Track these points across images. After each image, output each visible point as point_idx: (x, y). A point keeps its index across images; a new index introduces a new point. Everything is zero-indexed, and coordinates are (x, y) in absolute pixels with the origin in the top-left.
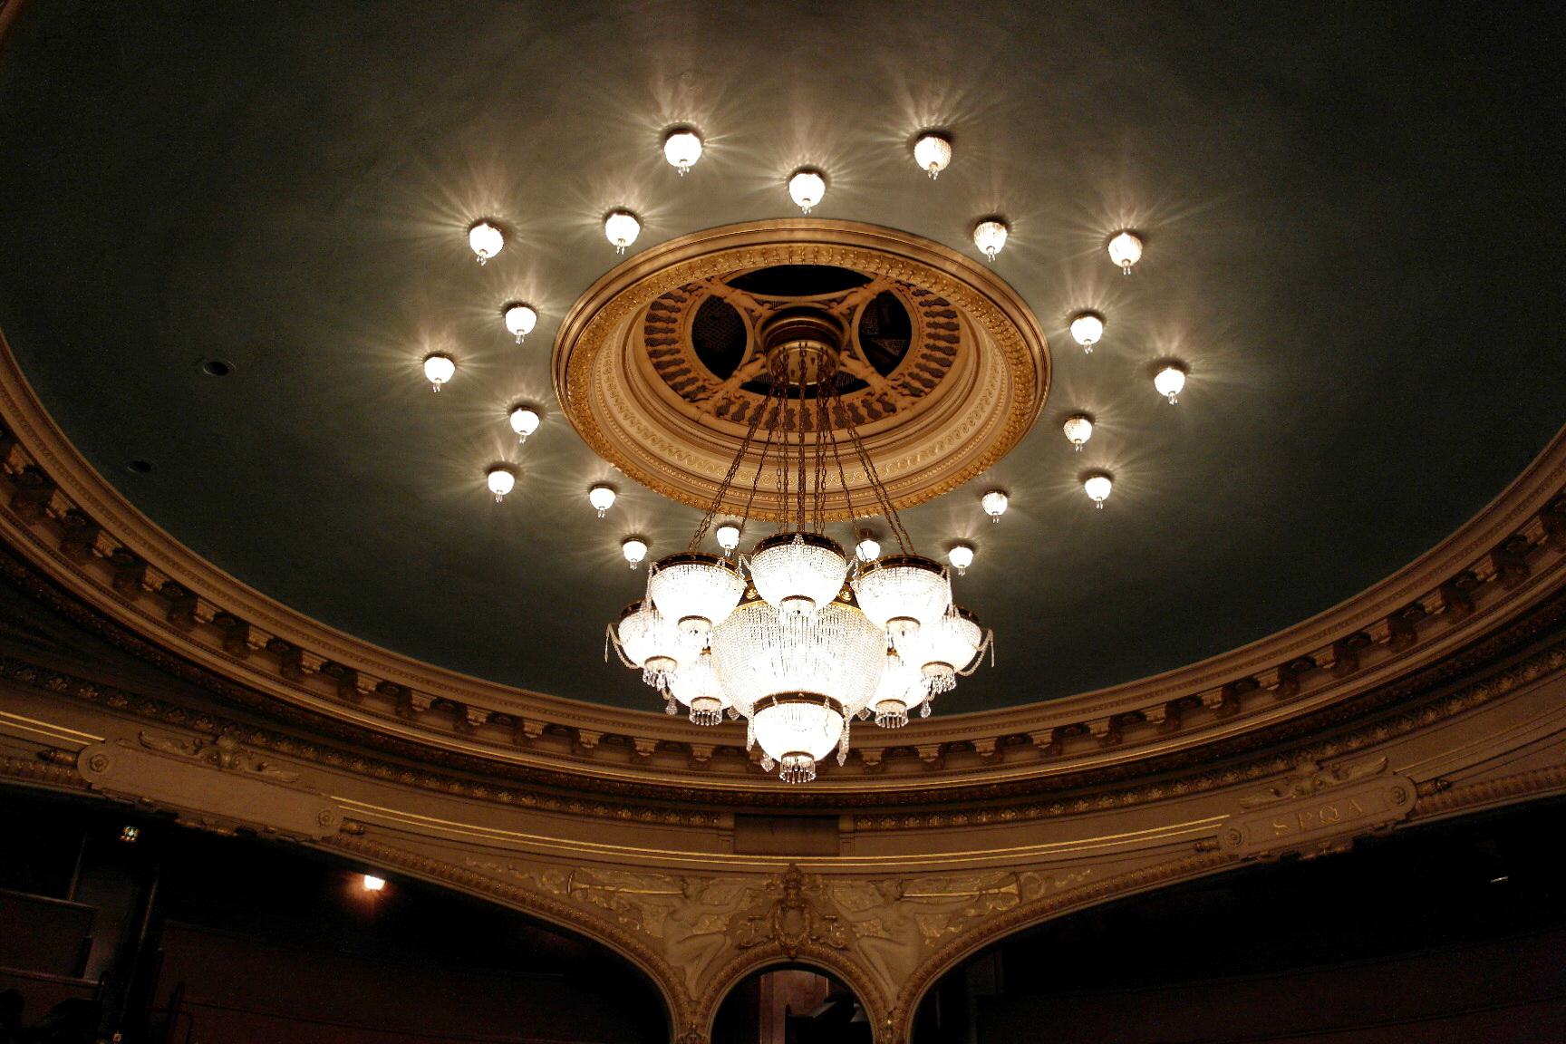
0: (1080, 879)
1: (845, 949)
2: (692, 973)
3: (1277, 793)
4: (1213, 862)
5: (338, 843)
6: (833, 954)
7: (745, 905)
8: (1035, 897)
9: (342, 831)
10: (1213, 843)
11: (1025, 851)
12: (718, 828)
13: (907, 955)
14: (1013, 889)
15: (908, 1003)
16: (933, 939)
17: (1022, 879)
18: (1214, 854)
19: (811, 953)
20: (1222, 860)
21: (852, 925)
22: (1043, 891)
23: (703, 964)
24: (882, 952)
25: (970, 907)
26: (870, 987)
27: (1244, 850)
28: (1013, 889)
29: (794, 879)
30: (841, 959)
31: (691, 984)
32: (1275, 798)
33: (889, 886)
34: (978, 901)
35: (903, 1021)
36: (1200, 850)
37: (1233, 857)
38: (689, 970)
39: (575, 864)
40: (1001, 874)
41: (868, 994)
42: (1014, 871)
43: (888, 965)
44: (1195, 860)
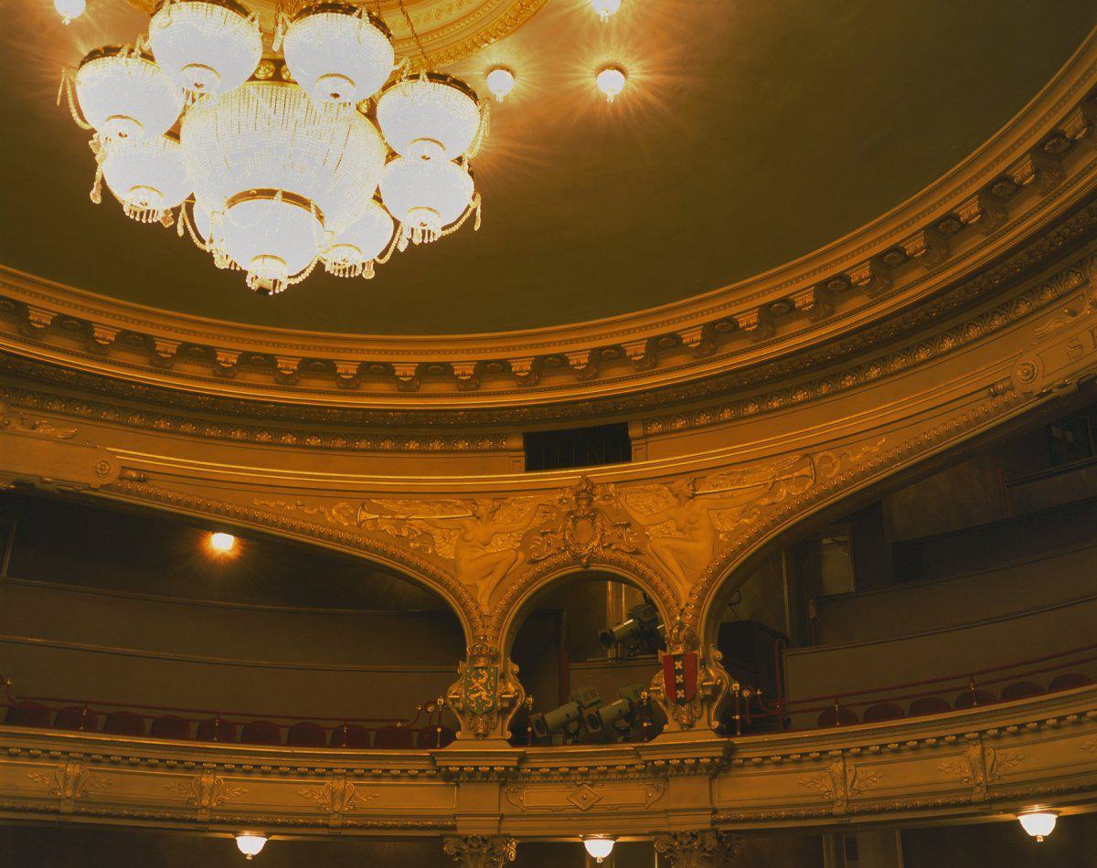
0: (875, 450)
1: (637, 552)
2: (484, 589)
3: (1073, 313)
4: (1008, 406)
5: (119, 490)
6: (625, 558)
7: (538, 521)
8: (829, 476)
9: (121, 478)
10: (1007, 384)
11: (817, 431)
12: (507, 450)
13: (701, 550)
14: (806, 471)
15: (701, 598)
16: (727, 533)
17: (817, 459)
18: (1010, 395)
19: (603, 560)
20: (1017, 402)
21: (643, 528)
22: (836, 470)
23: (494, 580)
24: (676, 551)
25: (765, 495)
26: (663, 586)
27: (1039, 385)
28: (806, 471)
29: (586, 491)
30: (633, 561)
31: (483, 600)
32: (1070, 320)
33: (682, 485)
34: (772, 489)
35: (696, 617)
36: (995, 395)
37: (1028, 395)
38: (482, 585)
39: (363, 497)
40: (795, 457)
41: (660, 594)
42: (807, 453)
43: (681, 564)
44: (990, 405)
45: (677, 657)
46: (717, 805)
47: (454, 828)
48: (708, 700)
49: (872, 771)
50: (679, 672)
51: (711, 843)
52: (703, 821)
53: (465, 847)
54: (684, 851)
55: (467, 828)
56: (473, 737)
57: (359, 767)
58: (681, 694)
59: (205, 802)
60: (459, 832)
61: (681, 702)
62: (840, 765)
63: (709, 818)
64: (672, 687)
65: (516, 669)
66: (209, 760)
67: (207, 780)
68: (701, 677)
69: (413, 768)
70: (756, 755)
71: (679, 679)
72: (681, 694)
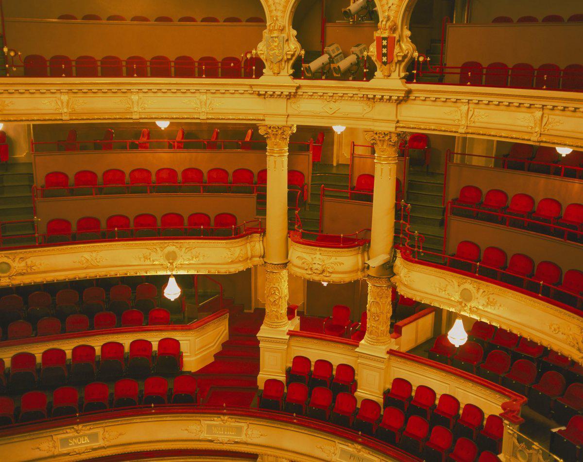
35: (397, 12)
45: (384, 39)
46: (399, 118)
47: (264, 120)
48: (399, 62)
49: (482, 112)
50: (384, 47)
51: (394, 139)
52: (391, 127)
53: (270, 131)
54: (380, 140)
55: (269, 121)
56: (271, 73)
57: (213, 89)
58: (384, 59)
59: (136, 109)
60: (266, 123)
61: (385, 63)
62: (466, 108)
63: (394, 125)
64: (380, 55)
65: (295, 32)
66: (134, 88)
67: (135, 97)
68: (397, 50)
69: (241, 89)
70: (422, 96)
71: (384, 51)
72: (384, 59)
